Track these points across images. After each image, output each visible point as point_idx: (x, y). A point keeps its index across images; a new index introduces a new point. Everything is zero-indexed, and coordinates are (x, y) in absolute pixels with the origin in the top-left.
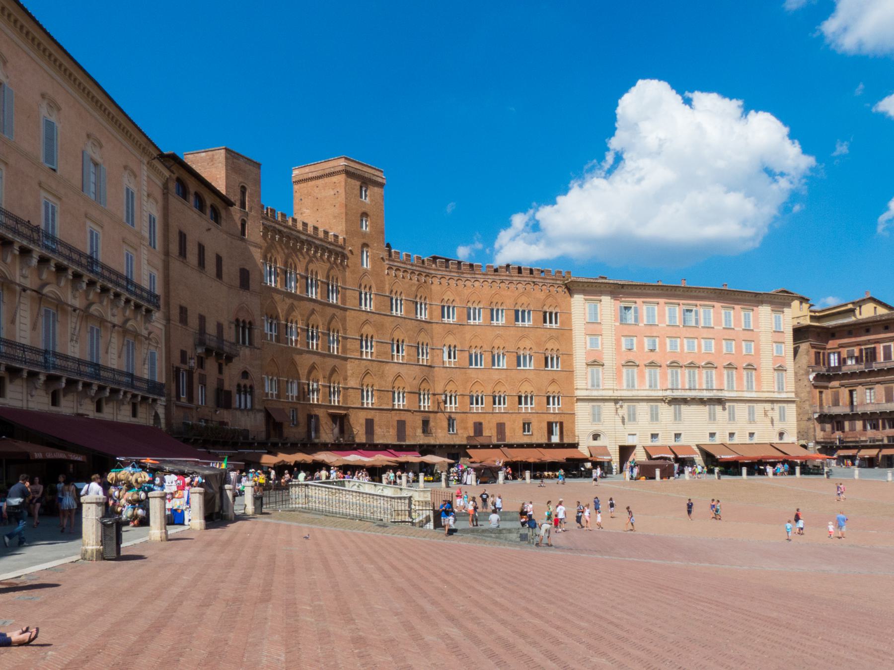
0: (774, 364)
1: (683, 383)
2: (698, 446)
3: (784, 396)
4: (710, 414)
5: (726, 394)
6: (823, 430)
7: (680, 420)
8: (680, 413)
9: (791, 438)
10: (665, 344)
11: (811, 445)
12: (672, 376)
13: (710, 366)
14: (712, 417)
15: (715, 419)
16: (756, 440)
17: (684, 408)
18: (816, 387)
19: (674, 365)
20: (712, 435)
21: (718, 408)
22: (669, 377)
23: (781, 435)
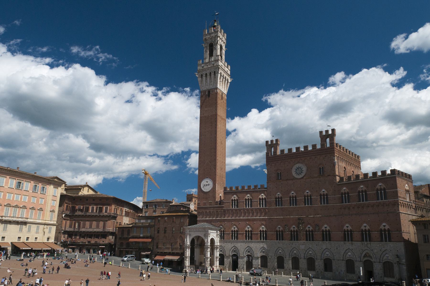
0: (51, 209)
1: (11, 214)
2: (11, 243)
3: (52, 222)
4: (20, 228)
5: (29, 220)
6: (64, 237)
7: (6, 231)
8: (6, 228)
9: (52, 240)
10: (6, 195)
11: (59, 243)
12: (6, 210)
13: (24, 207)
14: (21, 230)
15: (22, 231)
16: (38, 241)
17: (9, 226)
18: (64, 219)
19: (9, 205)
20: (19, 238)
21: (24, 226)
22: (5, 211)
23: (48, 239)
